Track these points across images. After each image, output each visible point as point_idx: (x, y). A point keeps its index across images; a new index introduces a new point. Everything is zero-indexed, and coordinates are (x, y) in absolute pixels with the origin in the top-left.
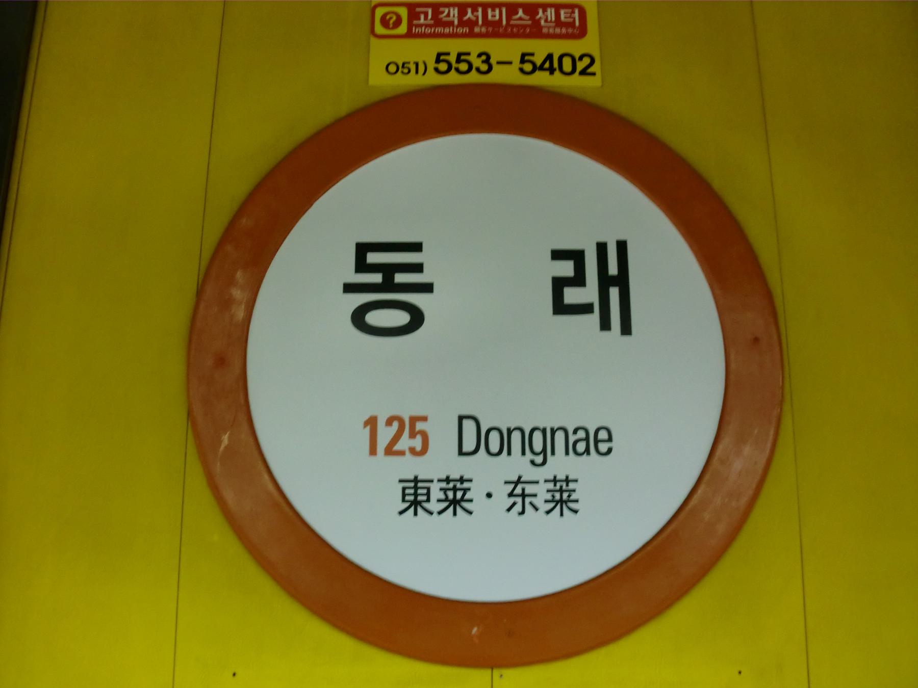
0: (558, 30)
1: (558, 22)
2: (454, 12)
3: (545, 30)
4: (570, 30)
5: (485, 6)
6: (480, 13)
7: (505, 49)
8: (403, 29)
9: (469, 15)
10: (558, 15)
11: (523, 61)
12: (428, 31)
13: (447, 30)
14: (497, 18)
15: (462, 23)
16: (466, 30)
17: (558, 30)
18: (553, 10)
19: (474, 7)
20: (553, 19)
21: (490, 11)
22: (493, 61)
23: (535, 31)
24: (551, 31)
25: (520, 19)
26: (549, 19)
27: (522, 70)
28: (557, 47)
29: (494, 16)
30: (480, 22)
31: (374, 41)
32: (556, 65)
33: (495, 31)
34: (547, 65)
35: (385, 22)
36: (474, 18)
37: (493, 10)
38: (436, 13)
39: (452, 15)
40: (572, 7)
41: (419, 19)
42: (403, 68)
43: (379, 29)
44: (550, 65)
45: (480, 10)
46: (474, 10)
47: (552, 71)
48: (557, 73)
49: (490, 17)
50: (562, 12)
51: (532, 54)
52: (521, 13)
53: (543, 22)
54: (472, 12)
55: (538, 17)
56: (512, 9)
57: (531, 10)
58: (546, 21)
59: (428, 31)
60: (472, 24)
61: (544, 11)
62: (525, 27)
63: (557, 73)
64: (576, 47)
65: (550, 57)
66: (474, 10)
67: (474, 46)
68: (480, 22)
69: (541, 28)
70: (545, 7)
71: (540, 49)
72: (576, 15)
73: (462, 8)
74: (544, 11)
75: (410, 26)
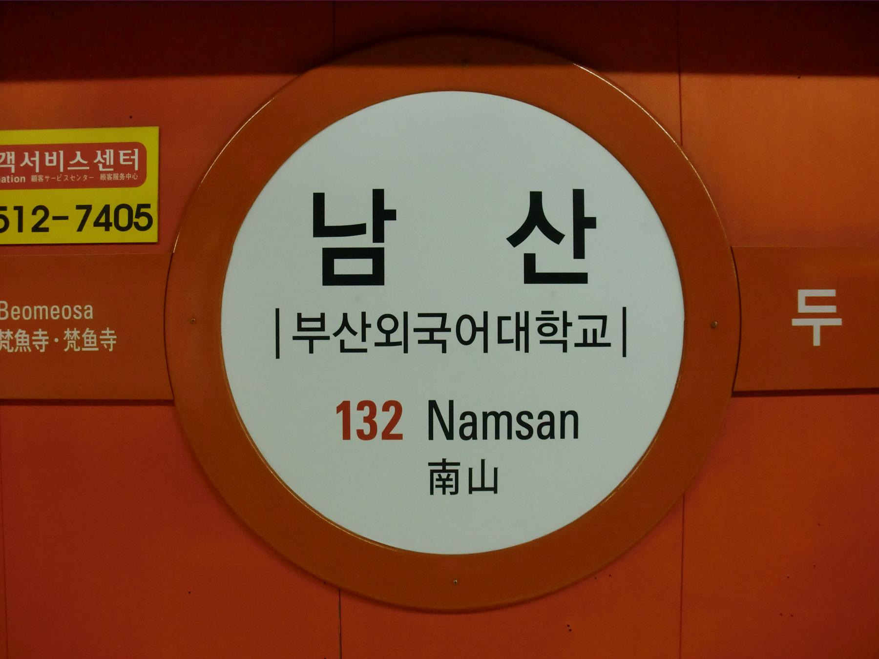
0: (116, 177)
1: (118, 167)
2: (11, 156)
3: (103, 177)
6: (37, 159)
9: (27, 160)
10: (117, 157)
14: (55, 164)
15: (20, 171)
16: (23, 179)
17: (116, 177)
18: (112, 151)
20: (112, 163)
21: (47, 154)
23: (93, 180)
24: (109, 177)
25: (79, 164)
26: (108, 163)
28: (113, 197)
29: (51, 161)
30: (37, 170)
32: (112, 220)
33: (54, 180)
34: (103, 220)
36: (31, 165)
37: (51, 155)
39: (9, 162)
44: (106, 219)
45: (37, 153)
46: (32, 155)
47: (107, 226)
48: (113, 228)
49: (47, 164)
50: (122, 153)
52: (79, 157)
53: (101, 169)
54: (30, 157)
55: (95, 161)
58: (105, 166)
60: (28, 171)
61: (103, 153)
63: (113, 228)
64: (133, 196)
65: (106, 209)
68: (37, 170)
70: (103, 147)
71: (98, 198)
74: (103, 153)
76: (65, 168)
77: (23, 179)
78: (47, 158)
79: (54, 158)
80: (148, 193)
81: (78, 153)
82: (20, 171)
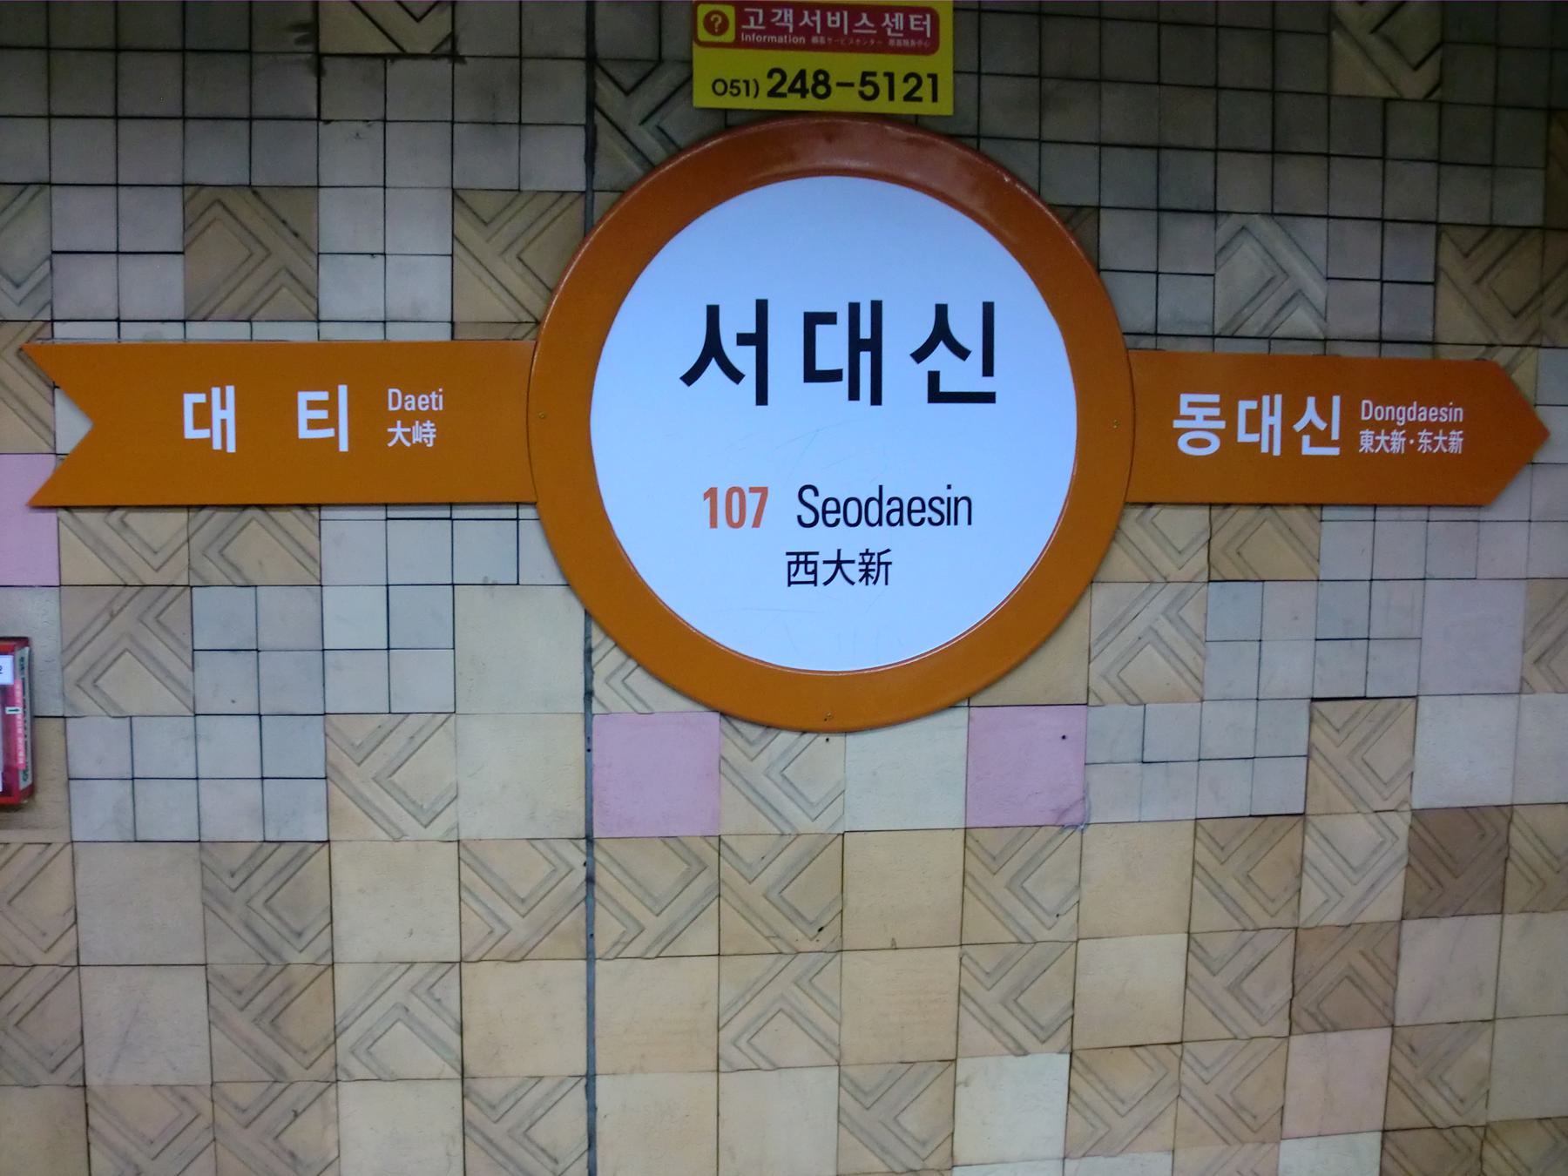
0: (906, 42)
2: (789, 14)
3: (892, 42)
4: (920, 42)
5: (825, 8)
6: (818, 18)
7: (844, 66)
8: (729, 36)
9: (806, 20)
11: (864, 83)
12: (759, 39)
13: (781, 40)
15: (798, 31)
16: (802, 39)
17: (906, 42)
19: (812, 8)
22: (832, 82)
23: (880, 44)
24: (899, 43)
25: (864, 27)
27: (862, 94)
31: (697, 50)
33: (837, 42)
35: (709, 26)
38: (769, 16)
40: (922, 11)
41: (748, 23)
42: (732, 87)
43: (703, 35)
46: (812, 14)
50: (912, 17)
51: (874, 74)
52: (865, 20)
56: (855, 12)
57: (876, 13)
58: (894, 30)
59: (759, 39)
60: (809, 31)
61: (892, 16)
62: (870, 36)
66: (812, 14)
67: (810, 62)
69: (886, 39)
70: (892, 10)
72: (928, 23)
73: (798, 10)
75: (738, 32)
76: (850, 29)
77: (802, 39)
78: (830, 18)
79: (838, 18)
80: (942, 62)
81: (865, 16)
82: (798, 31)
